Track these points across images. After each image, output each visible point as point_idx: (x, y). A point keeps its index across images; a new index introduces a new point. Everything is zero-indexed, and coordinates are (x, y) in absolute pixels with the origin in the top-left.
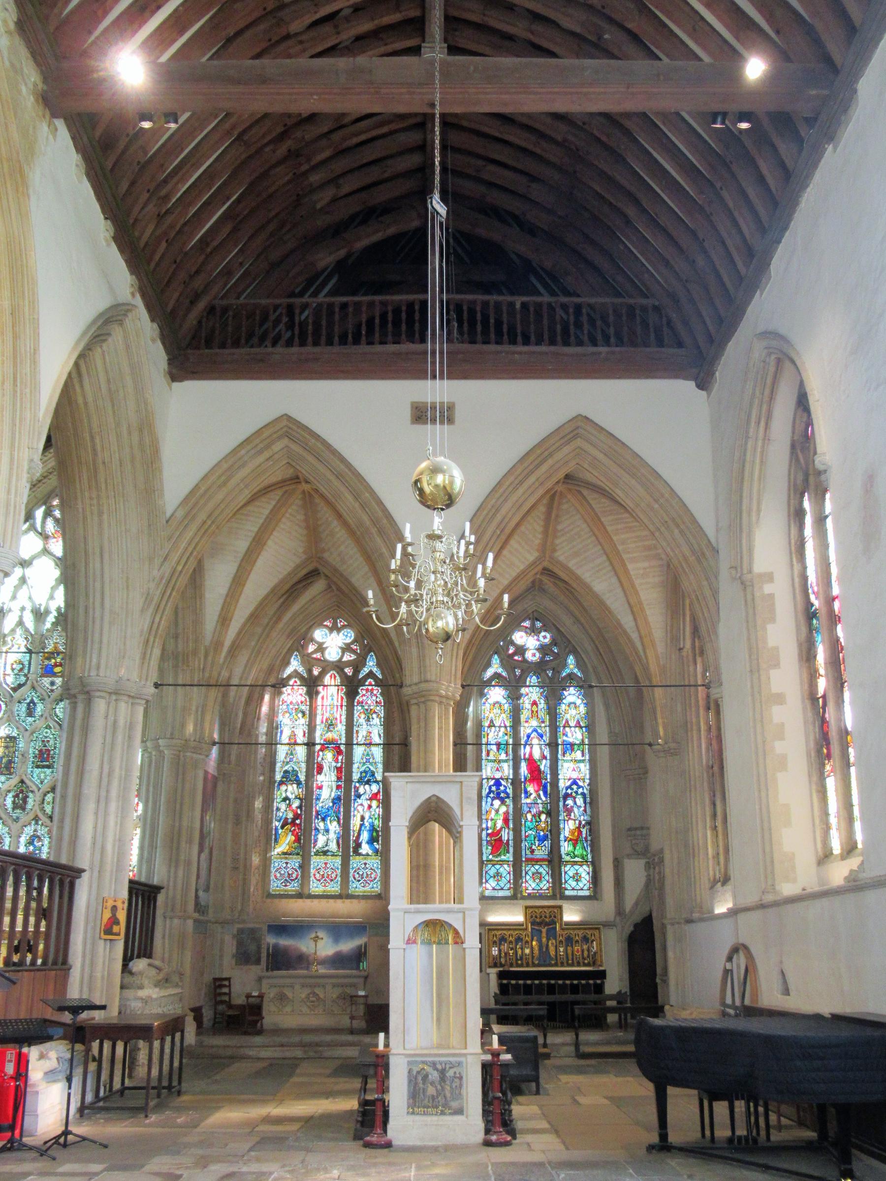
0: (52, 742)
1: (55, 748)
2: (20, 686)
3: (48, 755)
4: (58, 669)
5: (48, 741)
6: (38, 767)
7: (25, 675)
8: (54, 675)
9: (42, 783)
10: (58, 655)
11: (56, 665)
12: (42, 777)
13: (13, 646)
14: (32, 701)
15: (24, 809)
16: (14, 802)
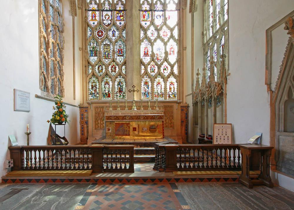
0: (122, 46)
1: (124, 48)
2: (109, 25)
3: (122, 51)
4: (122, 18)
5: (121, 46)
6: (118, 56)
7: (110, 20)
8: (121, 20)
9: (120, 62)
10: (121, 12)
11: (120, 16)
12: (120, 60)
13: (105, 8)
14: (114, 31)
15: (115, 72)
16: (111, 69)
